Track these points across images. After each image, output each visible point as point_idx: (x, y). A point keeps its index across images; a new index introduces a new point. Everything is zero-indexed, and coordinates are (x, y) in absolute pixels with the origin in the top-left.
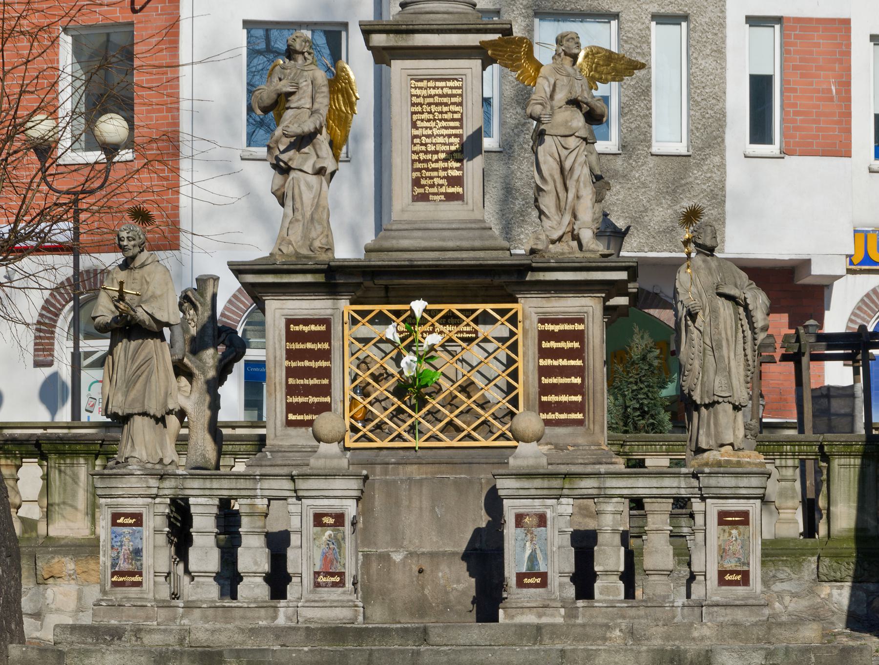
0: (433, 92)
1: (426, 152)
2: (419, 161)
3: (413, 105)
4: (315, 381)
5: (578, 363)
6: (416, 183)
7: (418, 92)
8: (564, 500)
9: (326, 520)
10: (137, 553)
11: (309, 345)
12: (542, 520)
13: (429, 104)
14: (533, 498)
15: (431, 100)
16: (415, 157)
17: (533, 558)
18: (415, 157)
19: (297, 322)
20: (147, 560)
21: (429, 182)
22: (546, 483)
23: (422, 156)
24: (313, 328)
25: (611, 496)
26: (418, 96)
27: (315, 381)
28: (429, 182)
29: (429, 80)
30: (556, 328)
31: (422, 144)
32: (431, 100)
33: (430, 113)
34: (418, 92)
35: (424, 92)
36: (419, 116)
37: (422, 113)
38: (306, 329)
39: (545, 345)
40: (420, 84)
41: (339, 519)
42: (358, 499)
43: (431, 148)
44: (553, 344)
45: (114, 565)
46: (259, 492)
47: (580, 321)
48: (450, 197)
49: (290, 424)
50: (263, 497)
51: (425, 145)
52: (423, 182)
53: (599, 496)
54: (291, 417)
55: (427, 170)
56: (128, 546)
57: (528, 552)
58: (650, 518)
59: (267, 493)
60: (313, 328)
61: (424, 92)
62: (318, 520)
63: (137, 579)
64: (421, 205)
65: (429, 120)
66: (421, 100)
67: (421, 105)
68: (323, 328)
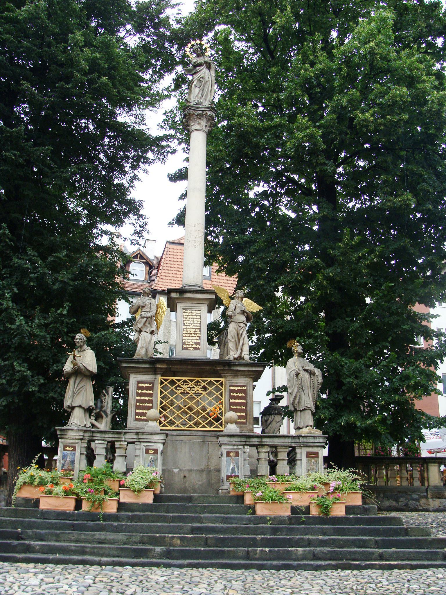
4: (147, 405)
5: (244, 401)
6: (184, 344)
8: (246, 447)
9: (150, 451)
10: (73, 462)
11: (145, 391)
12: (237, 454)
14: (234, 445)
17: (233, 470)
19: (141, 383)
20: (77, 465)
22: (239, 439)
24: (147, 385)
25: (264, 445)
27: (147, 405)
30: (236, 388)
38: (144, 385)
39: (232, 394)
41: (156, 451)
42: (164, 444)
44: (235, 394)
45: (62, 467)
46: (123, 439)
47: (245, 386)
48: (195, 349)
49: (136, 420)
50: (125, 441)
53: (259, 445)
54: (137, 417)
56: (69, 459)
57: (231, 467)
58: (279, 455)
59: (127, 440)
60: (147, 385)
62: (147, 451)
63: (72, 473)
68: (151, 385)
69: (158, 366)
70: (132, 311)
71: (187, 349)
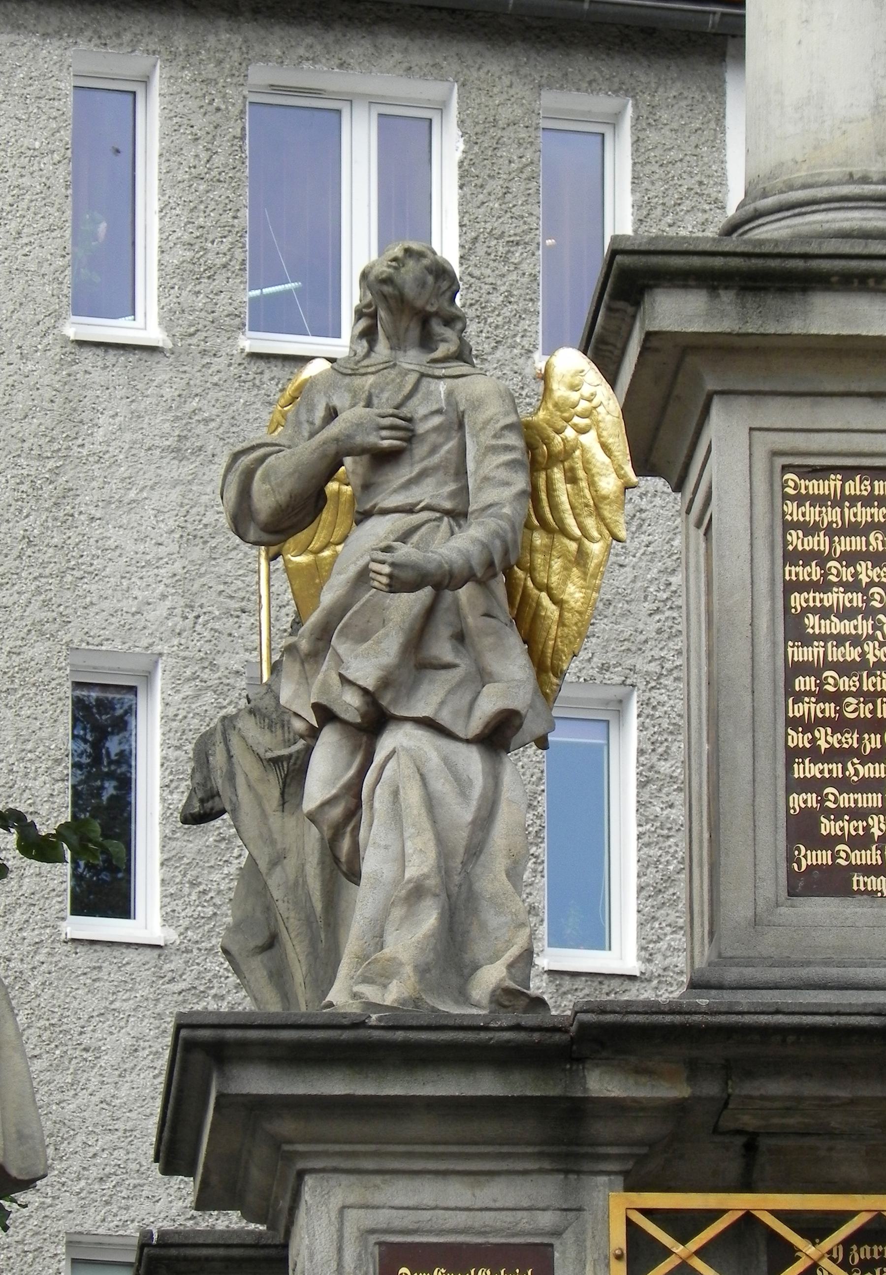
0: (862, 514)
1: (839, 725)
2: (814, 754)
3: (792, 557)
6: (803, 829)
7: (811, 514)
13: (850, 558)
15: (857, 543)
16: (799, 740)
18: (799, 740)
21: (851, 827)
23: (825, 739)
26: (809, 529)
28: (851, 827)
29: (847, 472)
31: (822, 696)
32: (857, 543)
33: (853, 586)
34: (811, 514)
35: (832, 515)
36: (814, 598)
37: (824, 586)
40: (816, 487)
43: (853, 709)
51: (838, 697)
52: (828, 827)
55: (844, 785)
61: (832, 515)
64: (819, 908)
65: (848, 614)
66: (818, 542)
67: (820, 558)
69: (602, 1084)
70: (265, 499)
71: (833, 882)
